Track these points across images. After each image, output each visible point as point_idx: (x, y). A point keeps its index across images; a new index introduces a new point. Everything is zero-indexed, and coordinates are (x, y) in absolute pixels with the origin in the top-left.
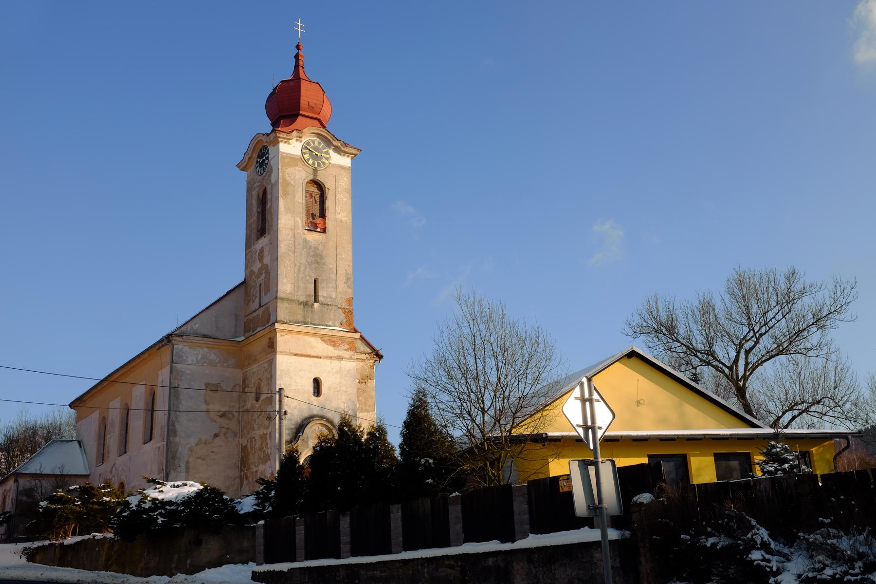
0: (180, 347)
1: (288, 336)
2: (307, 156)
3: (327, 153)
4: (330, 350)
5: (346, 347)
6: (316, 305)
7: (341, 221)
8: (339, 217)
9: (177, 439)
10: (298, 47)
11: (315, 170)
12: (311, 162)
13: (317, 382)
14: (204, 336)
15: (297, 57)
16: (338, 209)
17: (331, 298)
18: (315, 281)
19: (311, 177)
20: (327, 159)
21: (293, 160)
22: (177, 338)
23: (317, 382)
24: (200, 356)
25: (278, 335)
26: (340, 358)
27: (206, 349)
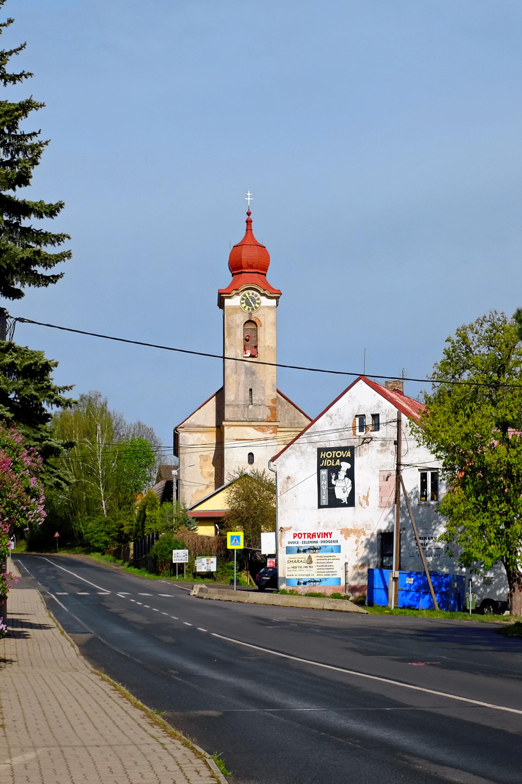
0: (184, 434)
1: (232, 428)
2: (244, 305)
3: (258, 299)
4: (261, 435)
5: (271, 431)
6: (251, 406)
7: (269, 346)
8: (267, 344)
9: (184, 490)
10: (249, 214)
11: (250, 314)
12: (246, 309)
13: (251, 455)
14: (199, 426)
15: (249, 222)
16: (267, 338)
17: (261, 400)
18: (251, 390)
19: (248, 319)
20: (259, 304)
21: (235, 309)
22: (181, 429)
23: (251, 455)
24: (196, 439)
25: (225, 428)
26: (266, 439)
27: (199, 434)
